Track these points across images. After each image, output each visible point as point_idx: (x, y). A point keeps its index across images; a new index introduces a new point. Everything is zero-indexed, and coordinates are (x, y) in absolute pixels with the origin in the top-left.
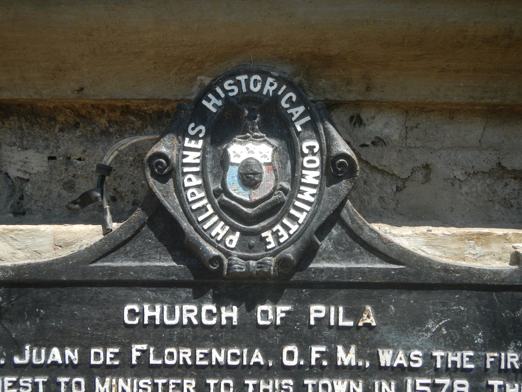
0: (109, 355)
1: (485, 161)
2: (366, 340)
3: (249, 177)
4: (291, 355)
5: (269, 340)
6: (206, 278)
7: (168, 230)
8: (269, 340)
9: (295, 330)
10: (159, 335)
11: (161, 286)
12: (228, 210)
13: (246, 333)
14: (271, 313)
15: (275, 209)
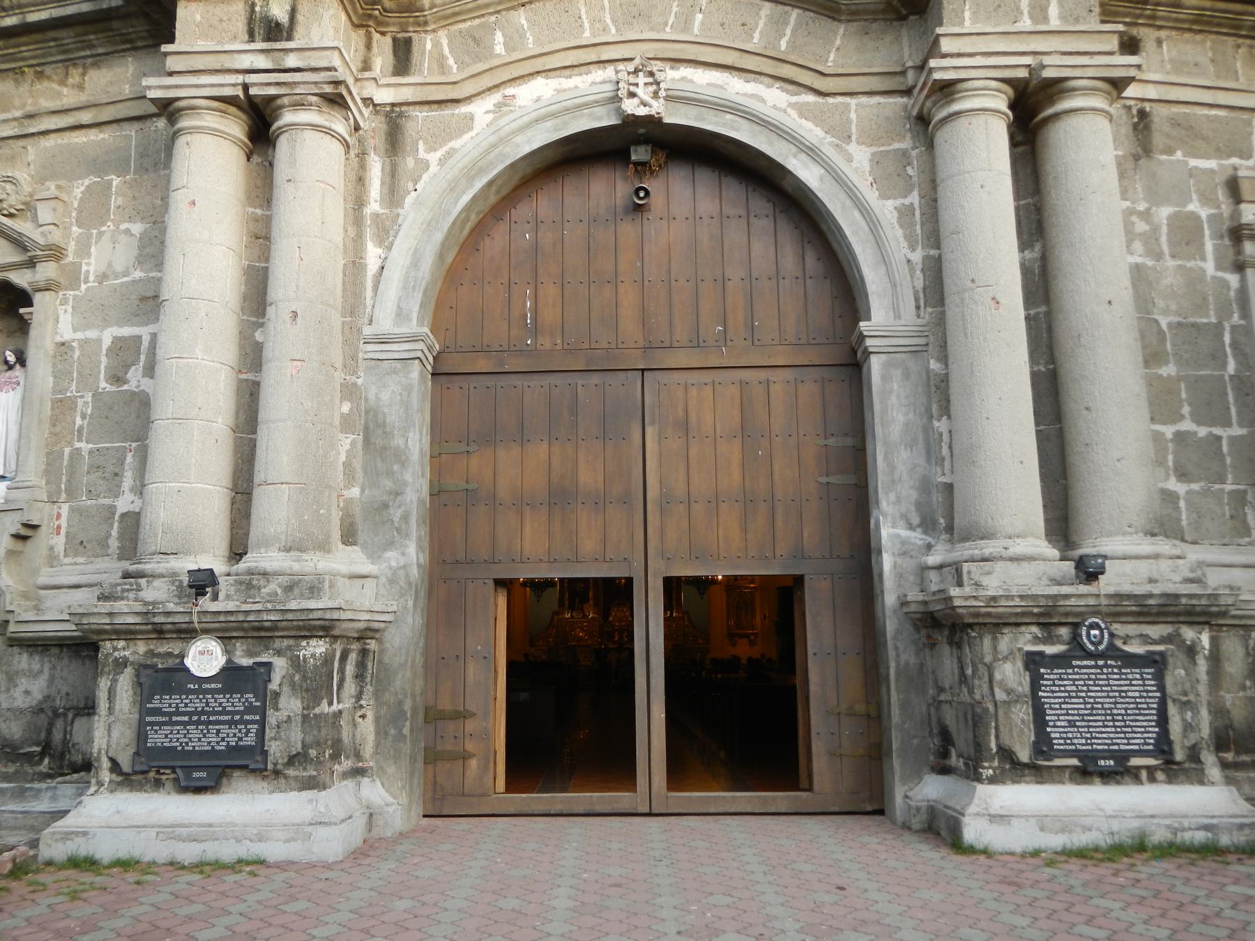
0: (1070, 671)
1: (1138, 633)
2: (1119, 668)
3: (1095, 636)
4: (1105, 670)
5: (1101, 667)
6: (1089, 655)
7: (1082, 647)
8: (1101, 667)
9: (1106, 666)
10: (1080, 667)
11: (1081, 658)
12: (1092, 643)
13: (1096, 666)
14: (1101, 663)
15: (1100, 643)
